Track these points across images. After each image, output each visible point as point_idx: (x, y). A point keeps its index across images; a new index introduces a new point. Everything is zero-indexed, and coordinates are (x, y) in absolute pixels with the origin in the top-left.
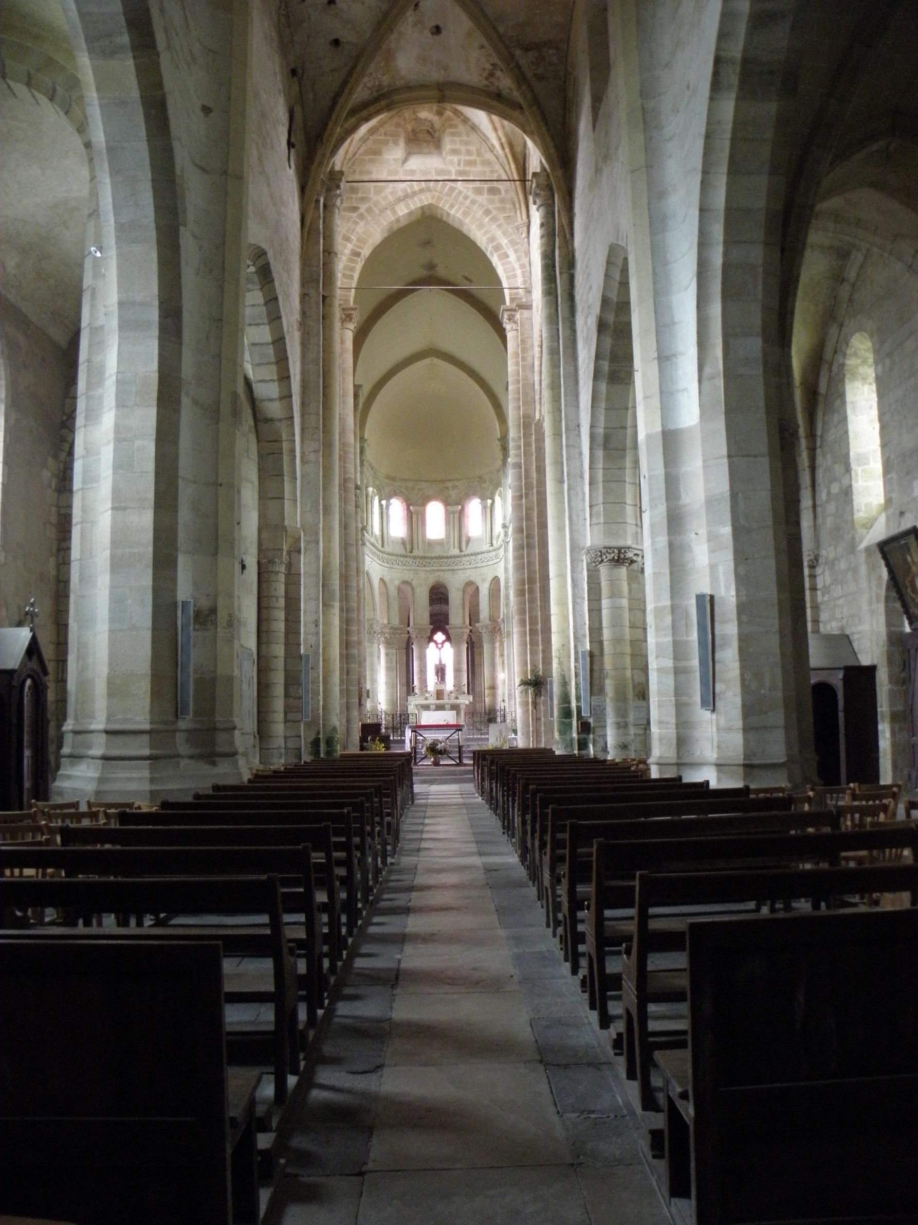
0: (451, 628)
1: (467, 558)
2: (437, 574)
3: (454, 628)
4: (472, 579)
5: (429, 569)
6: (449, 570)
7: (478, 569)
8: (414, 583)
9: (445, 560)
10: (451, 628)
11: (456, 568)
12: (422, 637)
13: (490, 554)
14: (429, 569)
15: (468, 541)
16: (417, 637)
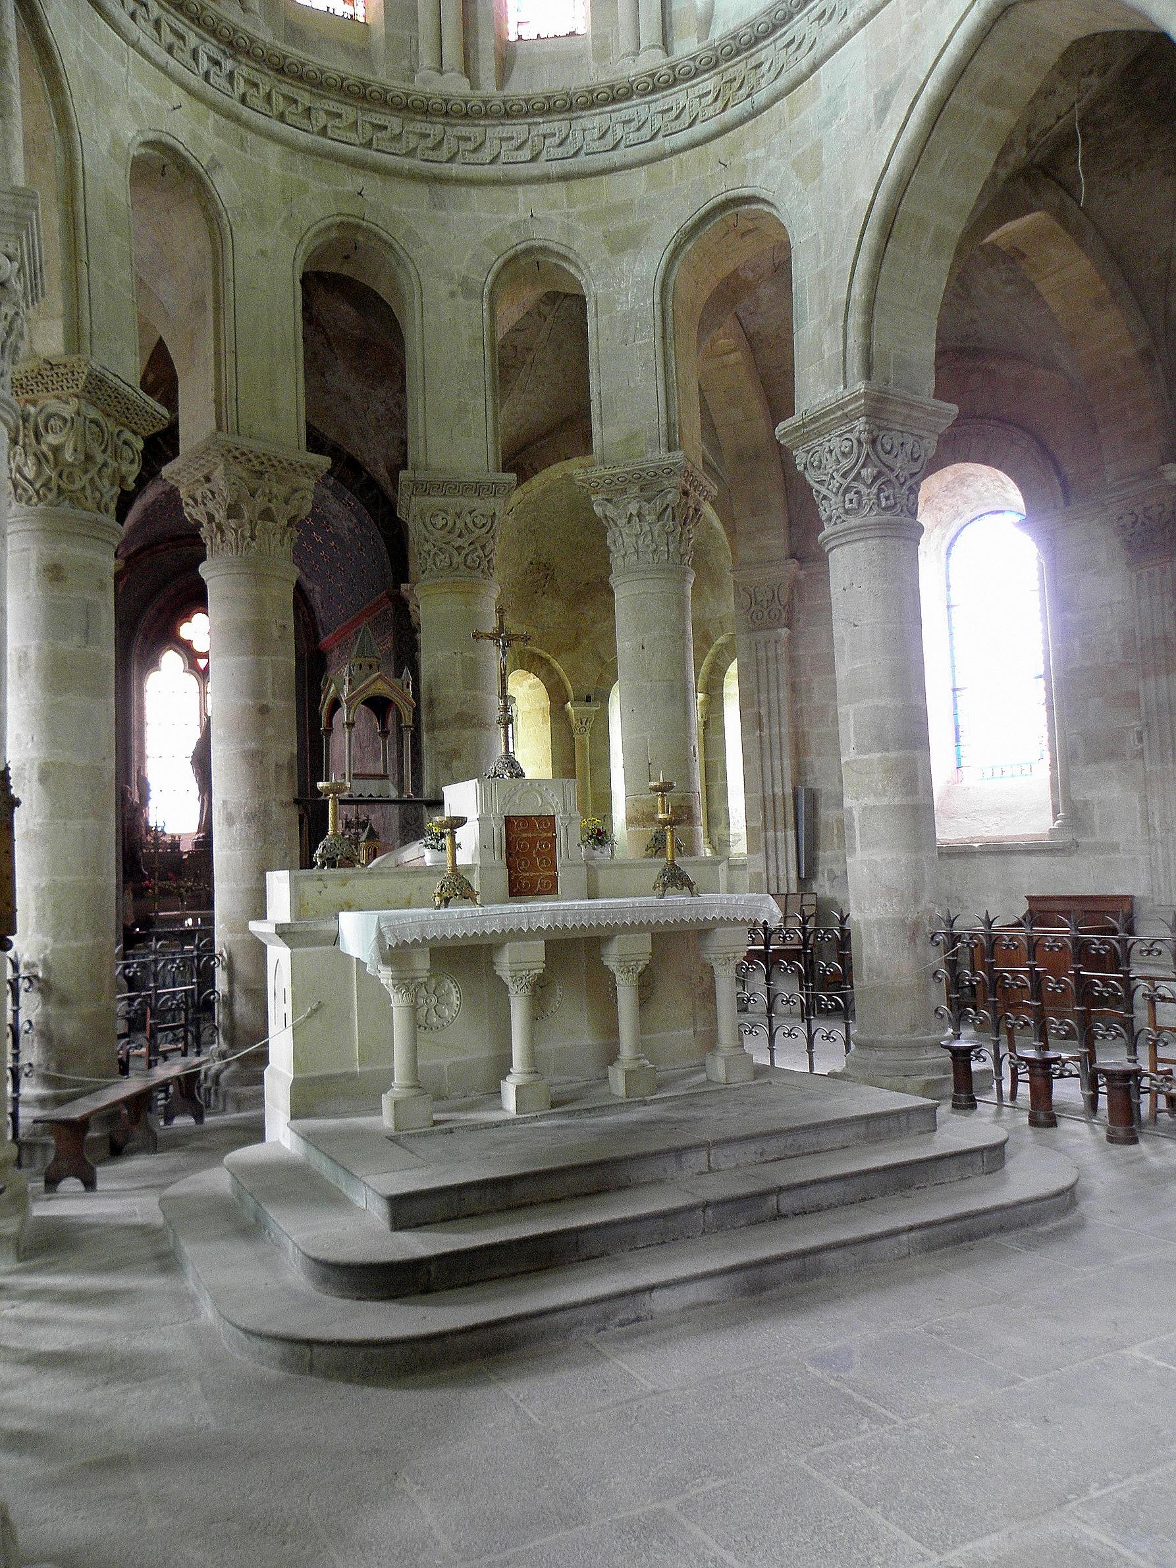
0: (424, 488)
1: (518, 129)
2: (353, 182)
3: (446, 487)
4: (550, 235)
5: (305, 139)
6: (414, 177)
7: (580, 188)
8: (224, 186)
9: (395, 123)
10: (424, 488)
11: (456, 169)
12: (267, 515)
13: (677, 97)
14: (305, 139)
15: (507, 57)
16: (233, 511)
